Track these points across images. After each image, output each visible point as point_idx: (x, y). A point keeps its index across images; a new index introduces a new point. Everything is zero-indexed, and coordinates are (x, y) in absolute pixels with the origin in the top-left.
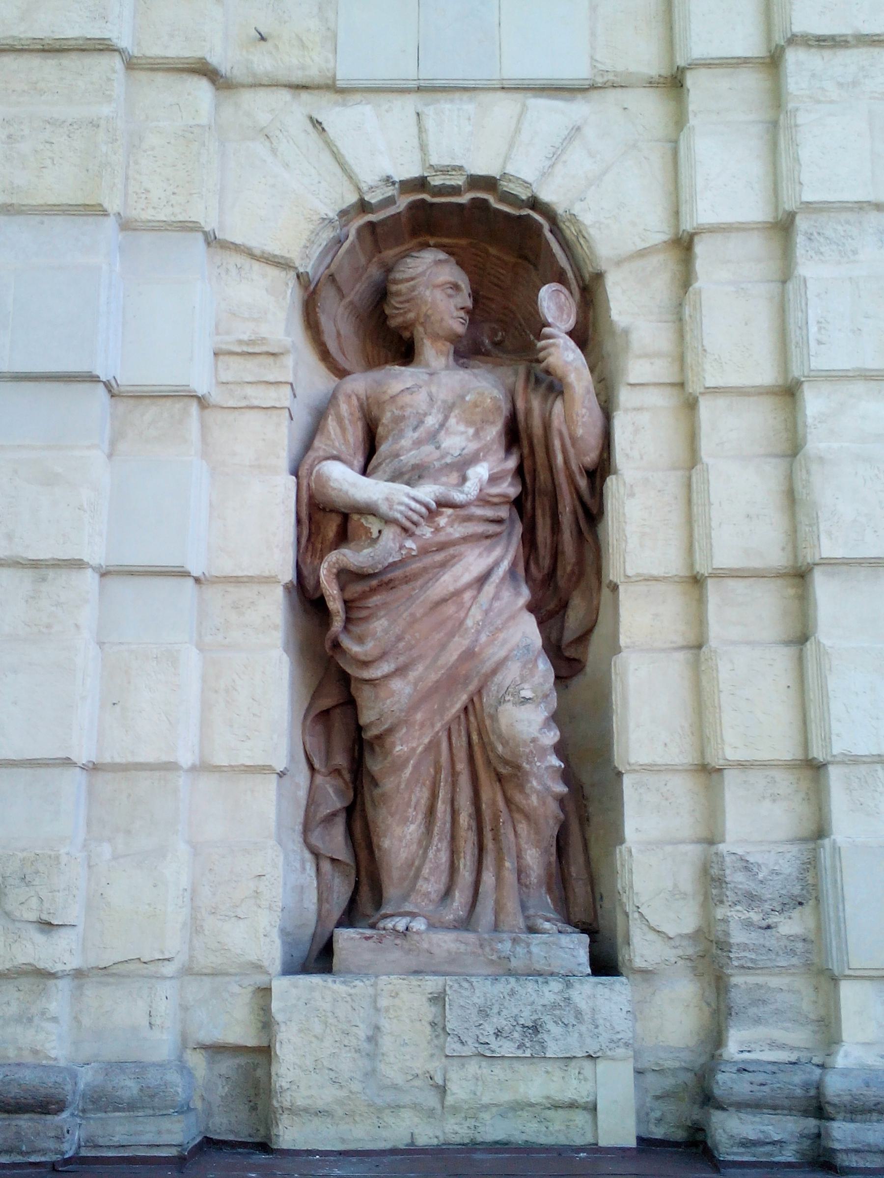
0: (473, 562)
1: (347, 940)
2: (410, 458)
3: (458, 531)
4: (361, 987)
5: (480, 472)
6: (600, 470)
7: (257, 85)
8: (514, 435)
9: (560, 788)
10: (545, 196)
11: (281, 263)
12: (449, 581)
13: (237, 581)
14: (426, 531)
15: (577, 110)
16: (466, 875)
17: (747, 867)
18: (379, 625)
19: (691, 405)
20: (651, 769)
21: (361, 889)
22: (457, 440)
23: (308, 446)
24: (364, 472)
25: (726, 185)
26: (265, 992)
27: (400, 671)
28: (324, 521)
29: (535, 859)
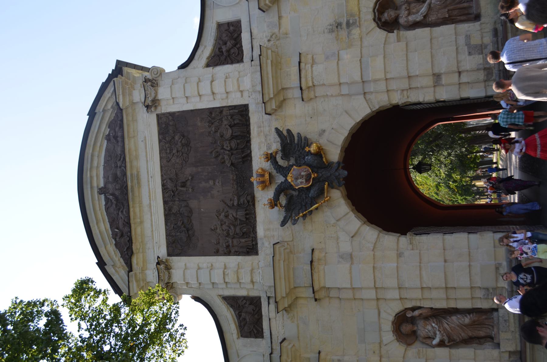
0: (446, 325)
1: (495, 341)
2: (433, 334)
3: (442, 328)
4: (501, 341)
5: (433, 325)
6: (432, 308)
7: (380, 353)
8: (426, 318)
9: (474, 314)
10: (394, 315)
11: (406, 350)
12: (449, 329)
13: (450, 355)
14: (442, 332)
15: (382, 311)
16: (486, 326)
17: (484, 295)
18: (455, 337)
19: (423, 299)
20: (472, 304)
21: (490, 338)
22: (429, 328)
23: (430, 346)
24: (434, 339)
25: (395, 294)
26: (502, 352)
27: (461, 335)
28: (441, 344)
29: (484, 317)
